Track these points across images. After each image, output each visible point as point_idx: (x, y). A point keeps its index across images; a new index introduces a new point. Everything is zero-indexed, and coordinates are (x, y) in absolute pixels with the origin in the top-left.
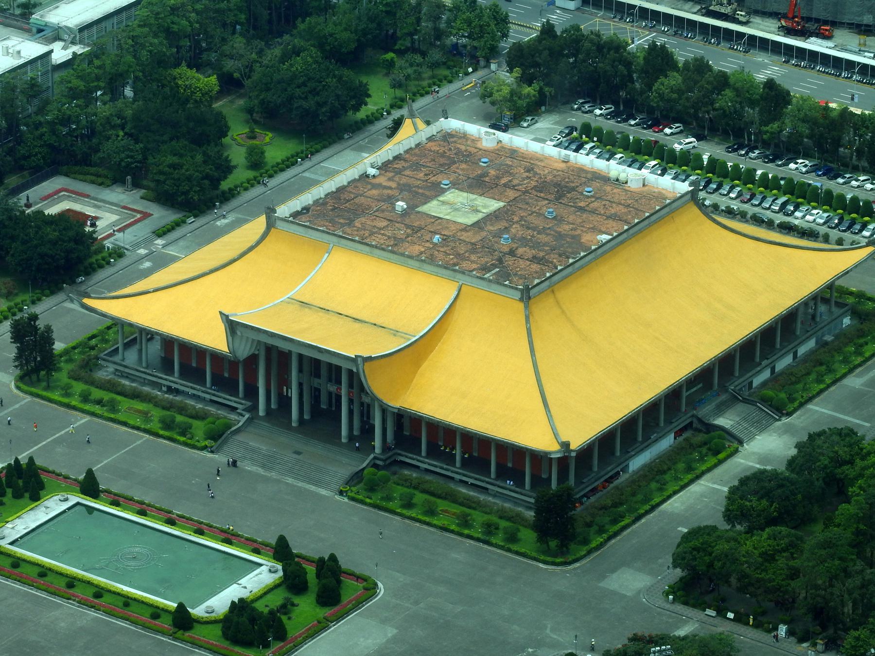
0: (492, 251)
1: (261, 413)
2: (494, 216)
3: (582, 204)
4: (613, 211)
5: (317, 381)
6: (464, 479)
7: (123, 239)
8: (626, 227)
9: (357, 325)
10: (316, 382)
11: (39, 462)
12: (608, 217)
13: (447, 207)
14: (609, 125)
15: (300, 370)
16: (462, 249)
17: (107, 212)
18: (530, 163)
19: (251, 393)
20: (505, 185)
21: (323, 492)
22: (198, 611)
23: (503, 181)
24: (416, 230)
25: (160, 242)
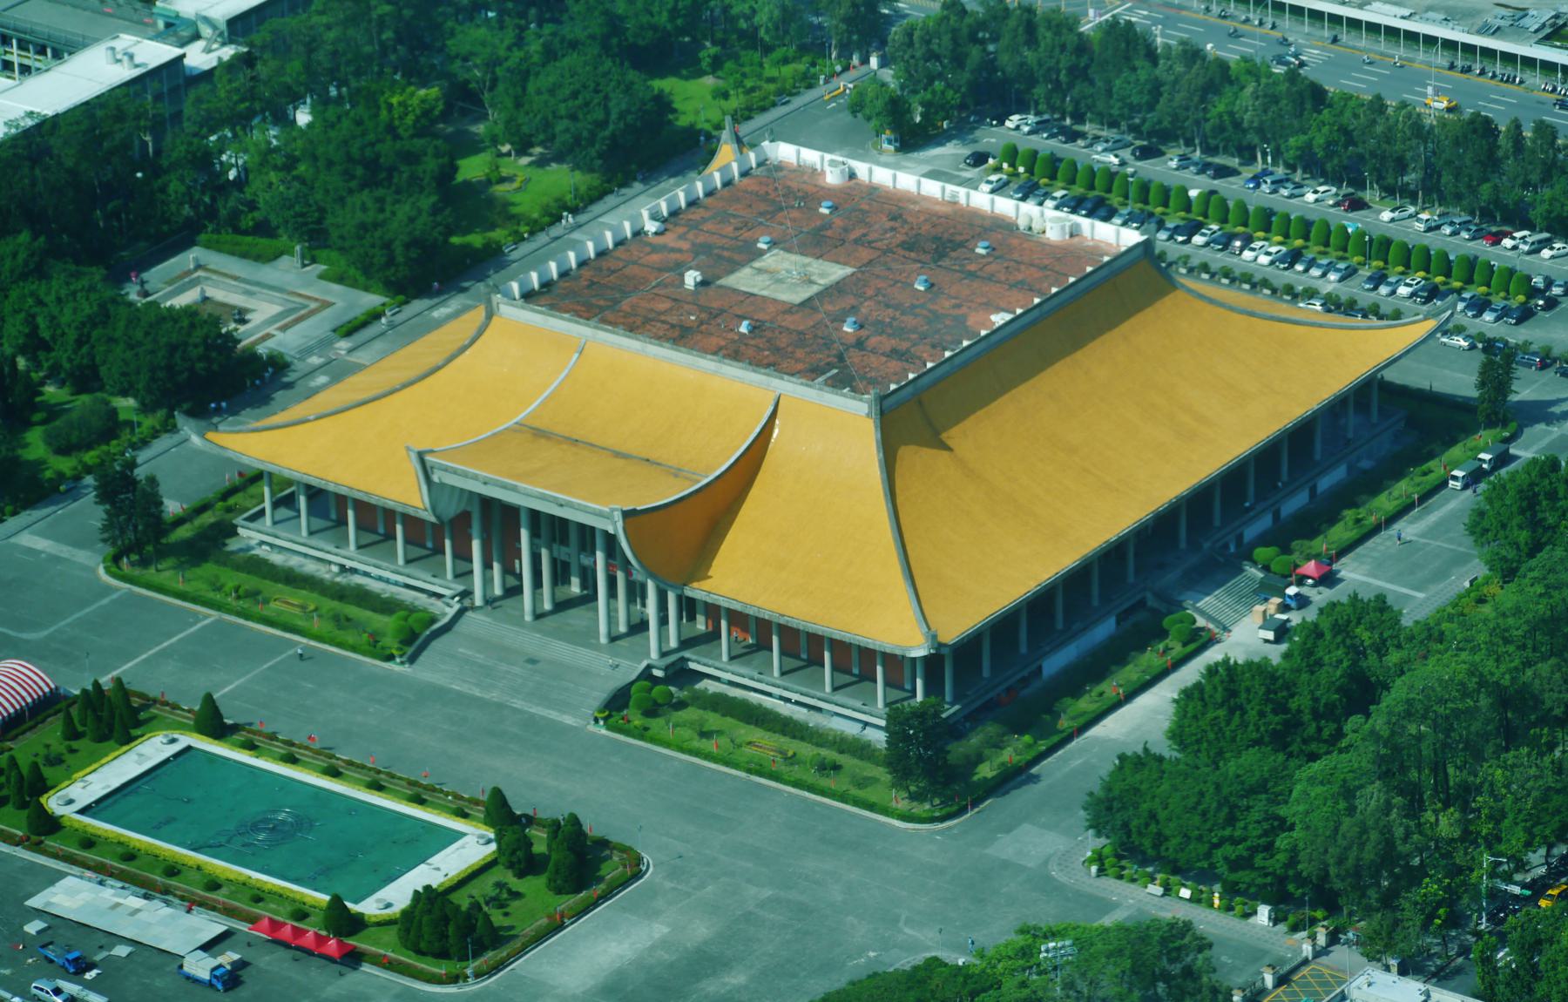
0: (828, 344)
1: (478, 602)
2: (838, 288)
3: (972, 267)
4: (1020, 277)
5: (564, 549)
6: (786, 694)
7: (285, 342)
8: (1037, 301)
9: (620, 462)
10: (563, 552)
11: (134, 685)
12: (1011, 286)
13: (765, 276)
14: (1046, 144)
15: (535, 534)
16: (783, 341)
17: (263, 297)
18: (895, 207)
19: (464, 575)
20: (856, 241)
21: (569, 720)
22: (369, 907)
23: (853, 236)
24: (715, 315)
25: (343, 345)
